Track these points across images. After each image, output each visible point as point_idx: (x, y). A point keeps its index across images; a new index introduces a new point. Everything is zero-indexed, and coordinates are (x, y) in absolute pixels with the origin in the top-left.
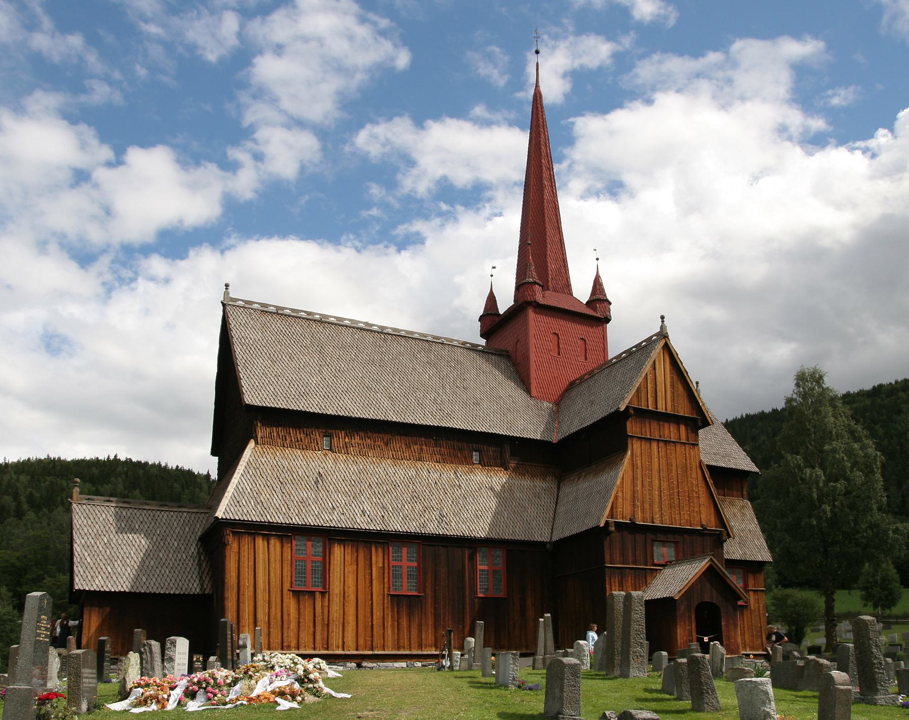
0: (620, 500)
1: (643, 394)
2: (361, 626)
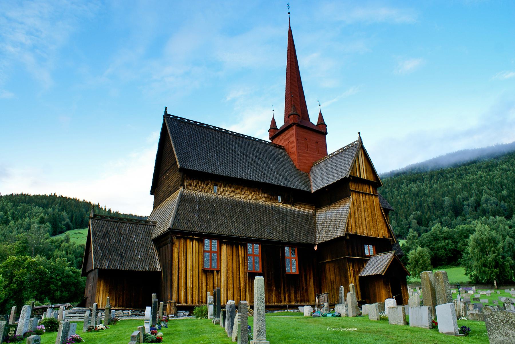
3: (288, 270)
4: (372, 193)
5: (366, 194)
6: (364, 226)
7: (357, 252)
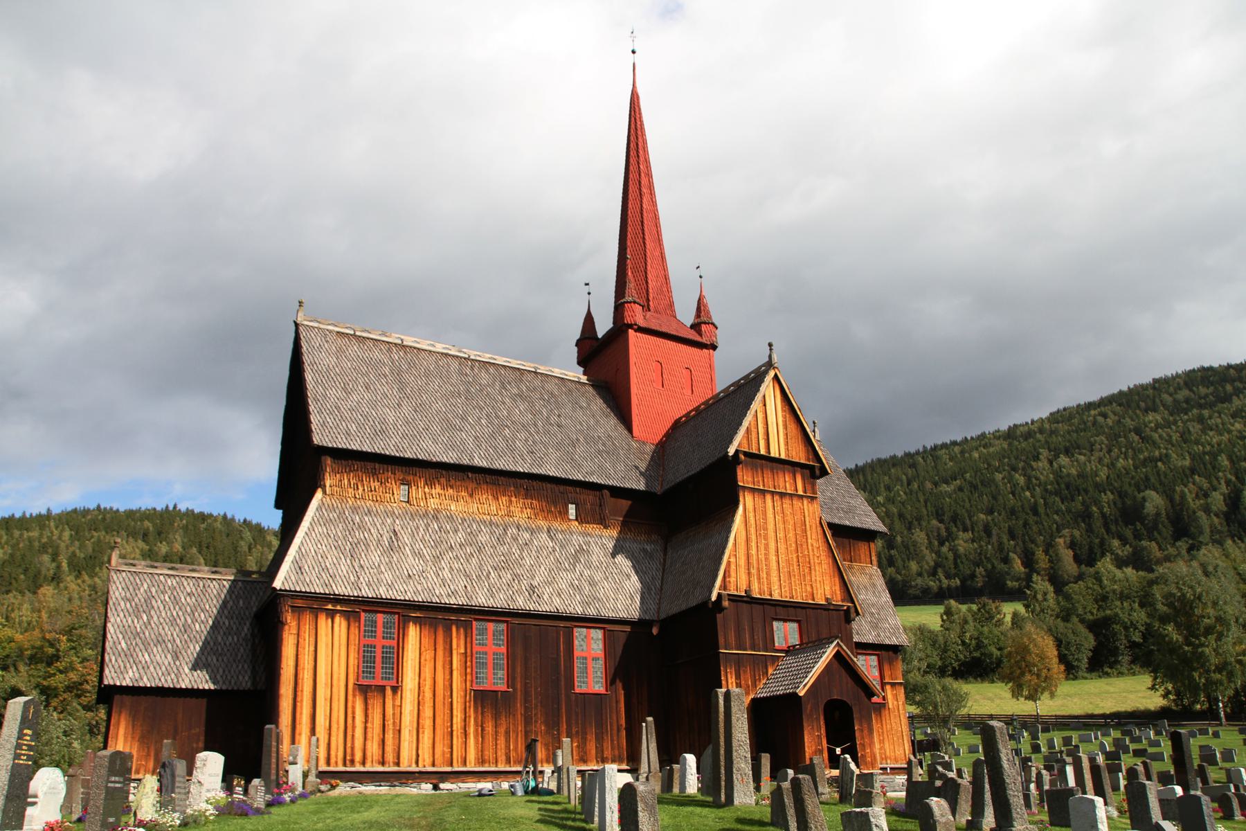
0: (733, 567)
1: (754, 435)
2: (438, 732)
3: (580, 687)
4: (800, 492)
5: (782, 495)
6: (774, 574)
7: (752, 637)
